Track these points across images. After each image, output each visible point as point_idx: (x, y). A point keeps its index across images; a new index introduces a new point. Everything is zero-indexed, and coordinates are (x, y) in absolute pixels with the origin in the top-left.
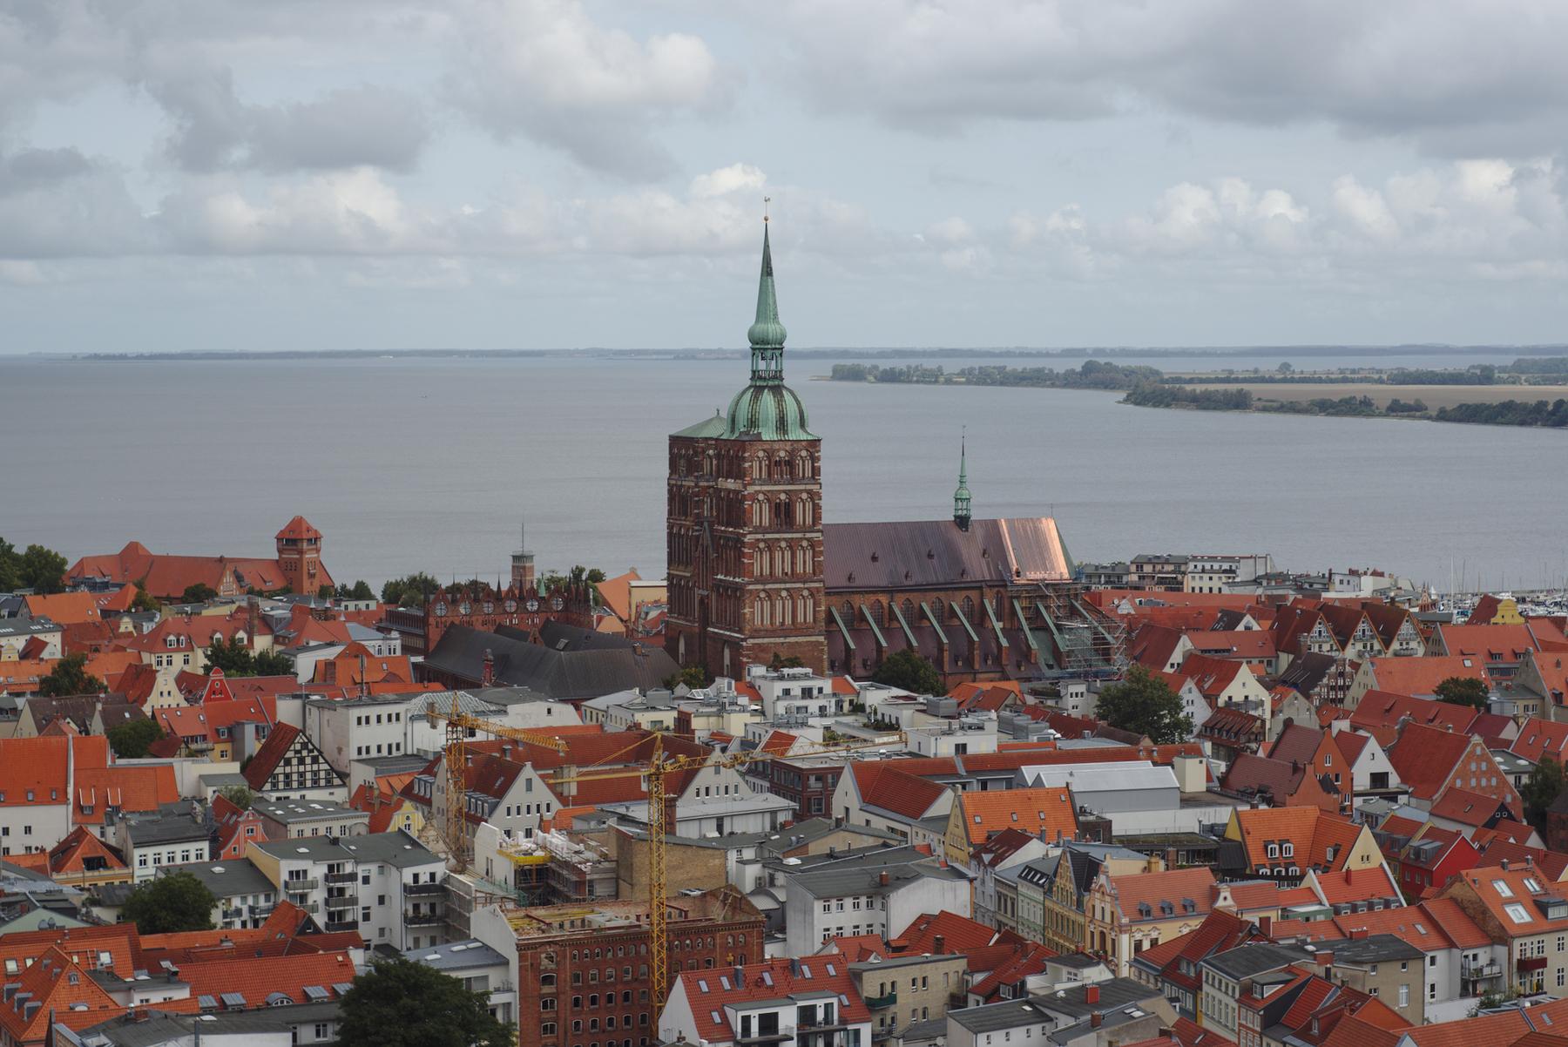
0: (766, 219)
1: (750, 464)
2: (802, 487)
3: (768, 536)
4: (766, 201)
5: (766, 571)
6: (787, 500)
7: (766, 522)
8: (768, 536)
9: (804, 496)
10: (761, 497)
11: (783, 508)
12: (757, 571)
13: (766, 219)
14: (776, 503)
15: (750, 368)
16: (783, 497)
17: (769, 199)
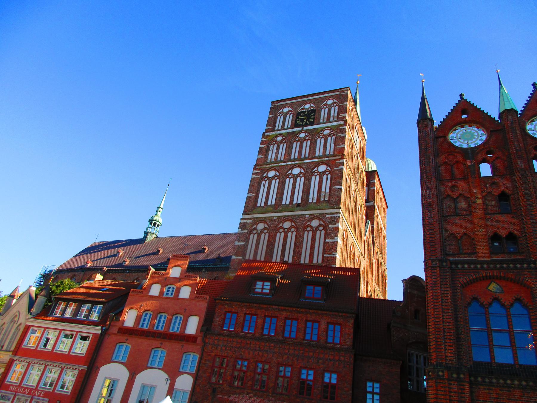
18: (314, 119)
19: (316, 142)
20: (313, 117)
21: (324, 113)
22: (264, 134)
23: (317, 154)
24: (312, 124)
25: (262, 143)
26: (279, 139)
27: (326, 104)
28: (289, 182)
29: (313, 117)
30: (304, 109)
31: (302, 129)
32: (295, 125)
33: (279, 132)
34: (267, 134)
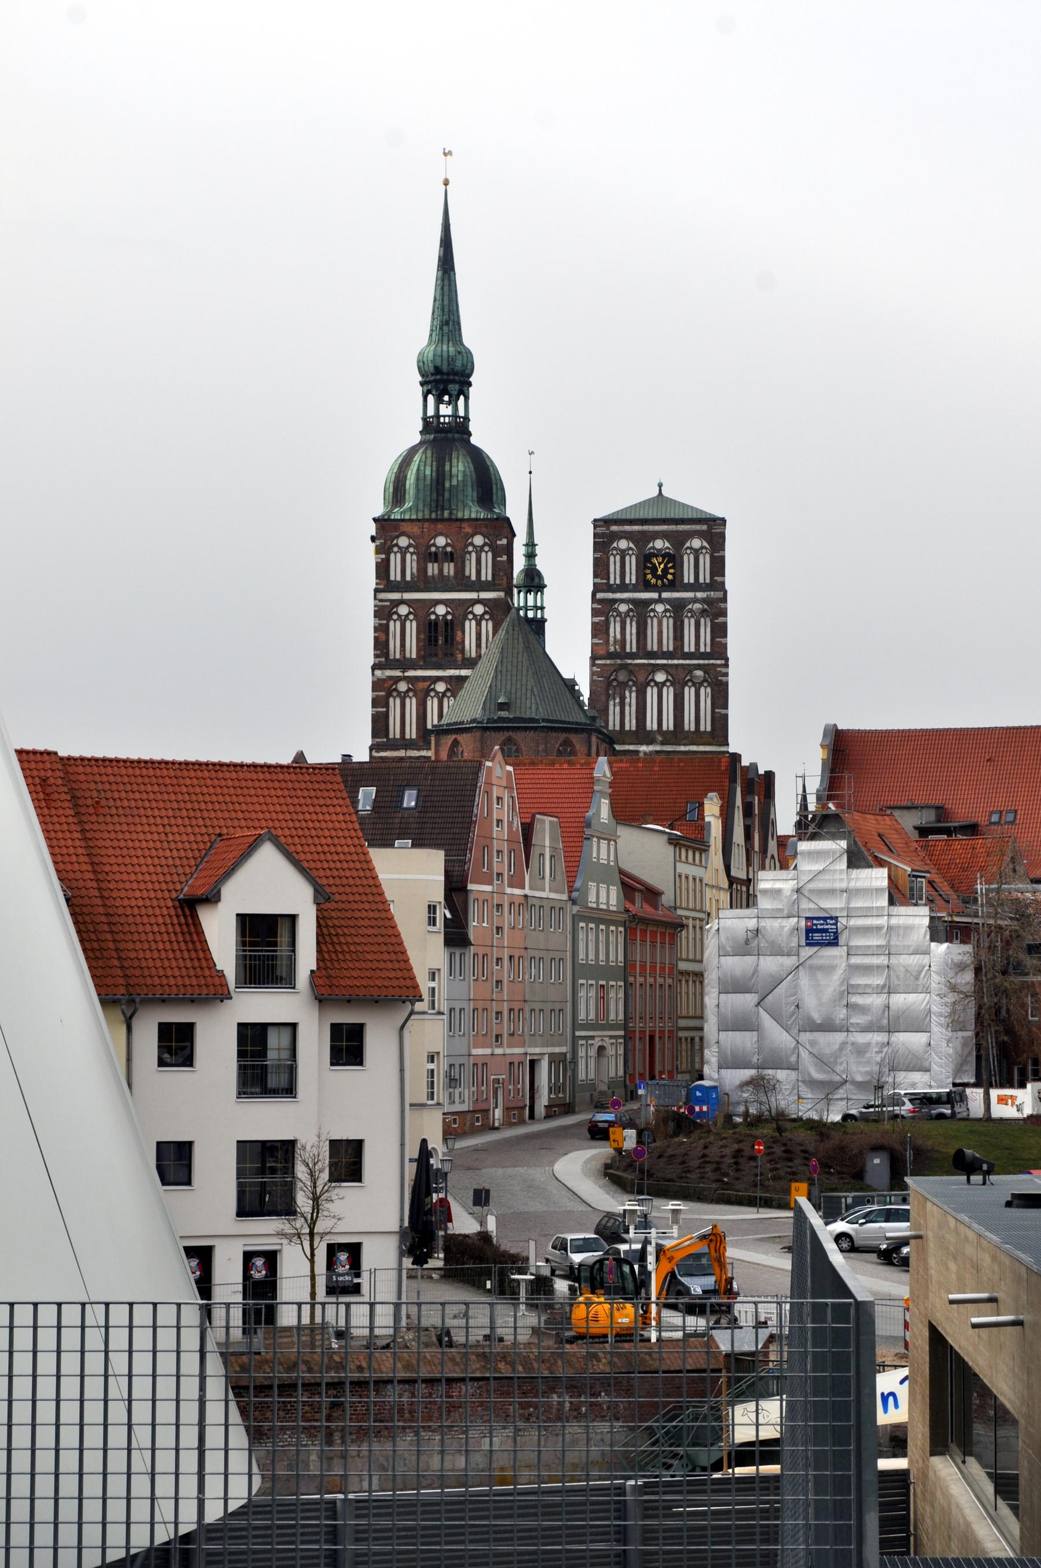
0: (446, 183)
1: (383, 556)
2: (473, 595)
3: (411, 673)
4: (445, 154)
5: (411, 732)
6: (449, 617)
7: (412, 651)
8: (411, 673)
9: (479, 609)
10: (403, 610)
11: (441, 628)
12: (394, 731)
13: (446, 183)
14: (430, 623)
15: (421, 415)
16: (441, 610)
17: (450, 153)
18: (673, 574)
19: (682, 622)
20: (671, 571)
21: (688, 561)
22: (594, 594)
23: (686, 650)
24: (672, 586)
25: (595, 613)
26: (623, 608)
27: (691, 548)
28: (651, 693)
29: (671, 571)
30: (654, 548)
31: (660, 596)
32: (647, 587)
33: (619, 596)
34: (600, 596)
